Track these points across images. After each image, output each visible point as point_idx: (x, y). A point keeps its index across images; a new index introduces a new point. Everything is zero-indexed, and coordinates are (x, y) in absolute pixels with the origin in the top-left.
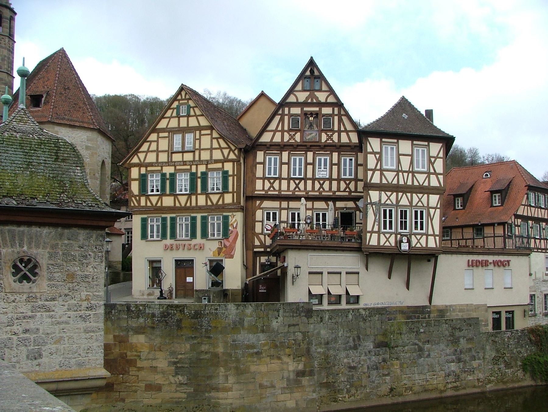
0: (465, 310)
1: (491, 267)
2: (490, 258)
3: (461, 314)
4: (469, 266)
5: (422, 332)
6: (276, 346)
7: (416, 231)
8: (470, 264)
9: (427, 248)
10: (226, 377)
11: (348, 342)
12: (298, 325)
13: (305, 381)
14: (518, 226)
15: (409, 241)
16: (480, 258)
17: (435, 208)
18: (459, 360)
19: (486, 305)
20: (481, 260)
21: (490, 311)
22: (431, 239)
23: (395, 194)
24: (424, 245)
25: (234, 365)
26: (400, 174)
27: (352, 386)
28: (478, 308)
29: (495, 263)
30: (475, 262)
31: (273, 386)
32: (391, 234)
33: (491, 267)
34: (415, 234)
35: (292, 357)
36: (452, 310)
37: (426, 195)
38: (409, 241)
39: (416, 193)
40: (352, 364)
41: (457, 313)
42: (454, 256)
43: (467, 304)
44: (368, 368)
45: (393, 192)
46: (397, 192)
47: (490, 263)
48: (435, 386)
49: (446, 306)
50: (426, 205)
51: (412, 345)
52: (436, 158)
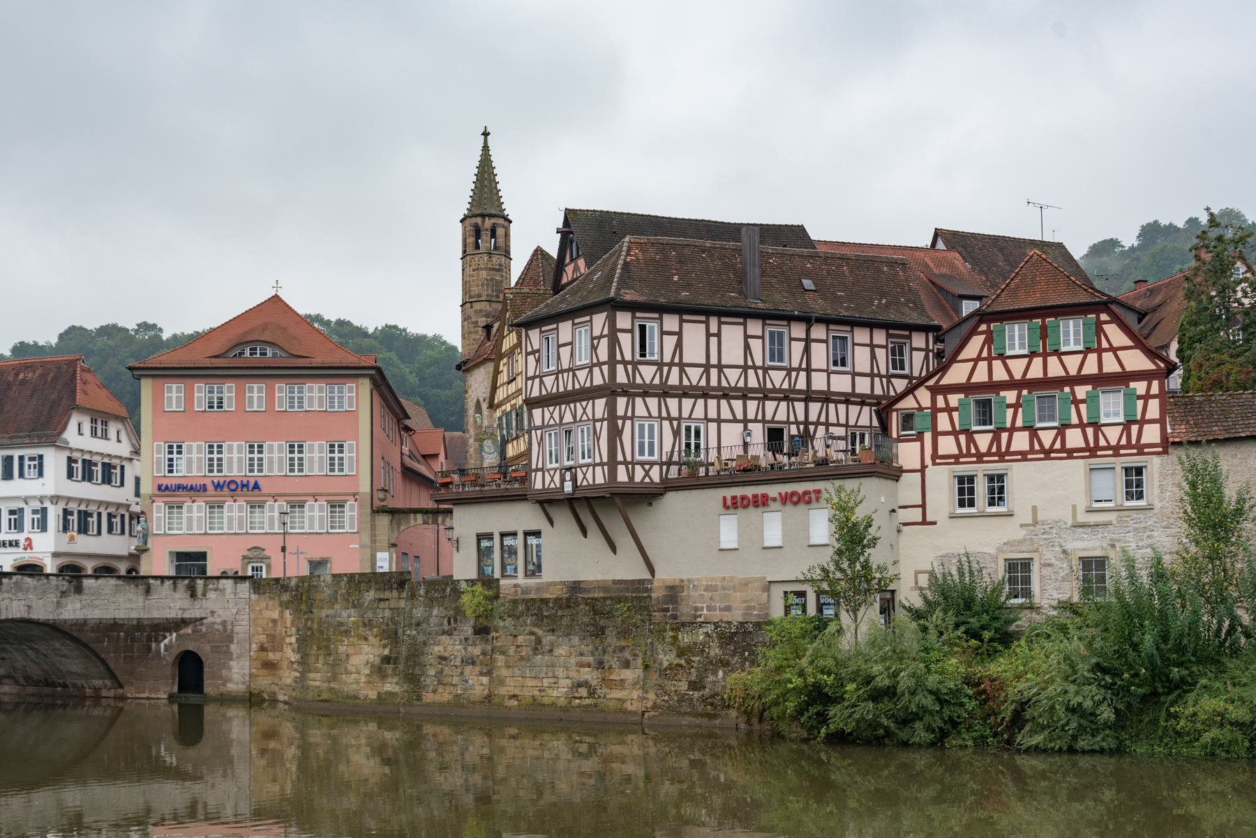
0: (720, 588)
1: (773, 505)
2: (773, 491)
3: (710, 594)
4: (726, 506)
5: (546, 616)
6: (365, 625)
7: (581, 461)
8: (729, 503)
9: (595, 487)
10: (318, 655)
11: (442, 624)
12: (388, 599)
13: (389, 668)
14: (949, 410)
15: (574, 479)
16: (749, 491)
17: (602, 420)
18: (600, 665)
19: (764, 578)
20: (801, 493)
21: (777, 592)
22: (598, 469)
23: (558, 407)
24: (591, 483)
25: (325, 643)
26: (560, 375)
27: (440, 683)
28: (746, 584)
29: (785, 499)
30: (739, 500)
31: (358, 673)
32: (555, 470)
33: (777, 505)
34: (581, 467)
35: (378, 638)
36: (691, 586)
37: (591, 401)
38: (574, 479)
39: (580, 401)
40: (446, 655)
41: (702, 592)
42: (680, 493)
43: (724, 578)
44: (462, 661)
45: (555, 405)
46: (560, 404)
47: (774, 499)
48: (553, 699)
49: (682, 581)
50: (591, 418)
51: (527, 635)
52: (601, 336)
